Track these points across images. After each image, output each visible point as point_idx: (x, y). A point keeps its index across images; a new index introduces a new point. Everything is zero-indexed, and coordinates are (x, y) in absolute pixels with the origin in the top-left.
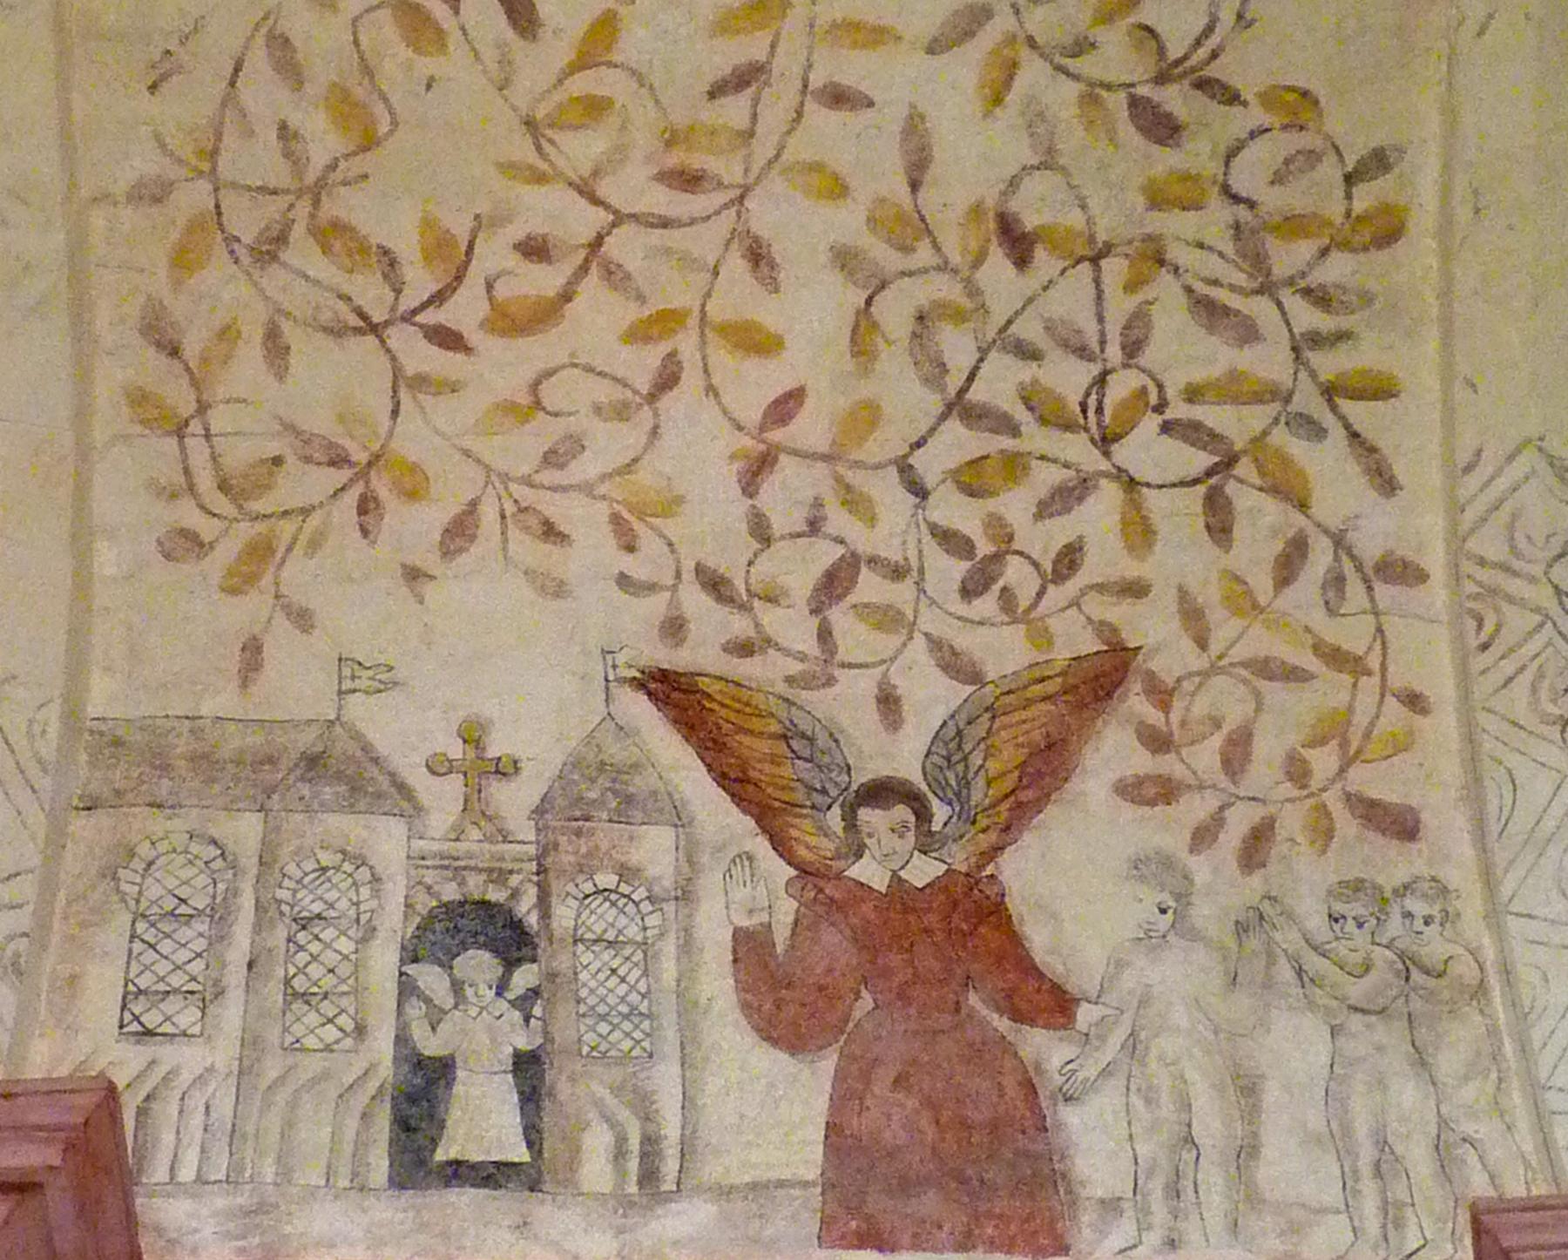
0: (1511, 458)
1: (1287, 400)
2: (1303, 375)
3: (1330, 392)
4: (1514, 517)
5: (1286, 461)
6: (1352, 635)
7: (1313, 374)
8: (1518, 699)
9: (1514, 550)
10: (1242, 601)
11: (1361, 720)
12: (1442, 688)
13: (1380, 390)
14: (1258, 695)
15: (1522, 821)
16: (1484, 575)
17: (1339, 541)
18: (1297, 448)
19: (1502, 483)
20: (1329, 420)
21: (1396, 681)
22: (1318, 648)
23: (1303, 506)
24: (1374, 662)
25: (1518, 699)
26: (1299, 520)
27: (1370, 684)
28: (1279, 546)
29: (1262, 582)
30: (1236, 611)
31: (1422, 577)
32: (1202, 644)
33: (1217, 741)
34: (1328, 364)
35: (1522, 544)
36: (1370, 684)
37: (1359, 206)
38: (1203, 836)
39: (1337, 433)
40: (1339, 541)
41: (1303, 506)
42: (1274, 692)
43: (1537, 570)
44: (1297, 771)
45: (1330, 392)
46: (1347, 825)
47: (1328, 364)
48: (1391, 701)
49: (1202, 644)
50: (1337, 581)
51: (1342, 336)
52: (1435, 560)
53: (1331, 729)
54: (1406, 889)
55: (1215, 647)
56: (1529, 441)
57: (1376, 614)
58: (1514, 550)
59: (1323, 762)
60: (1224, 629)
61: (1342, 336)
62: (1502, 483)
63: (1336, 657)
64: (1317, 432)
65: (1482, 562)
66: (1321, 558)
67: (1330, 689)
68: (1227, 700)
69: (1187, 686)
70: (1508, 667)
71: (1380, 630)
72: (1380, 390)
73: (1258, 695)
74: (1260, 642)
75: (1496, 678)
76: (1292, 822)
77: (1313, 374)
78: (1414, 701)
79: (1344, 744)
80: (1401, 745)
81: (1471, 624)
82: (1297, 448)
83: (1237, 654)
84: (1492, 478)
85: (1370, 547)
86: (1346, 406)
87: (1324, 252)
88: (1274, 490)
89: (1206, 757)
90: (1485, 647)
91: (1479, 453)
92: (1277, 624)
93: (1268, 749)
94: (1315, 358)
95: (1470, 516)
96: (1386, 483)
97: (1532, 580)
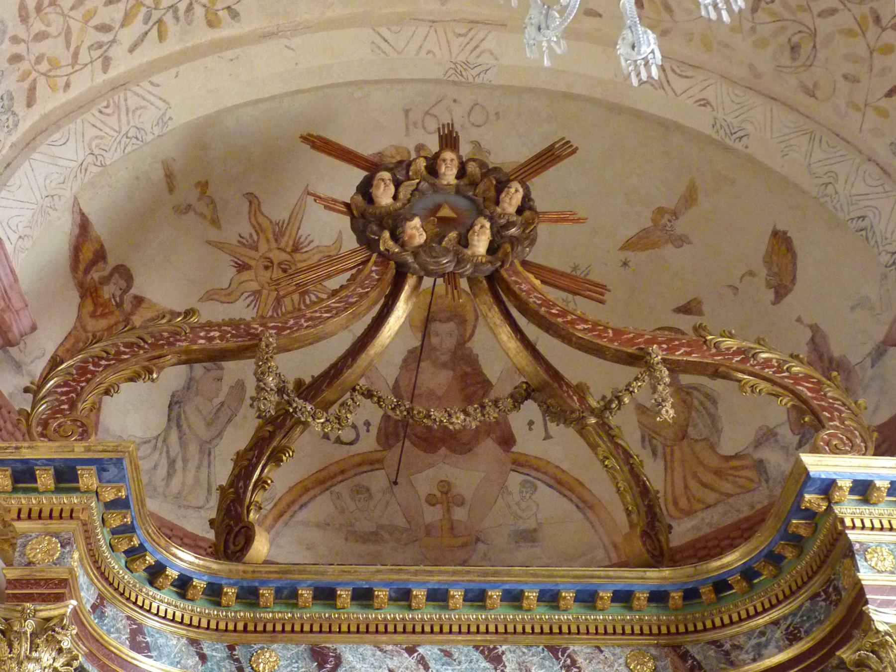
0: (161, 99)
1: (156, 9)
2: (164, 11)
3: (160, 21)
4: (144, 107)
5: (136, 15)
6: (84, 57)
7: (164, 14)
8: (91, 132)
9: (134, 111)
10: (88, 17)
11: (59, 72)
12: (73, 93)
13: (161, 37)
14: (60, 34)
15: (57, 151)
16: (122, 102)
17: (113, 41)
18: (140, 17)
19: (152, 98)
20: (151, 23)
21: (72, 77)
22: (78, 48)
23: (122, 26)
24: (77, 67)
25: (91, 132)
26: (117, 26)
27: (70, 70)
28: (108, 22)
29: (95, 22)
30: (84, 16)
31: (105, 72)
32: (71, 9)
33: (43, 28)
34: (169, 18)
35: (138, 112)
36: (70, 70)
37: (220, 13)
38: (15, 40)
39: (146, 28)
40: (113, 41)
41: (122, 26)
42: (61, 40)
43: (132, 124)
44: (39, 60)
45: (160, 21)
46: (26, 85)
47: (169, 18)
48: (66, 78)
49: (71, 9)
50: (100, 45)
51: (177, 19)
52: (112, 73)
53: (54, 64)
54: (14, 114)
55: (72, 13)
56: (168, 104)
57: (91, 62)
58: (134, 111)
59: (44, 67)
60: (78, 14)
61: (177, 19)
62: (152, 98)
63: (76, 55)
64: (146, 22)
65: (126, 100)
66: (105, 38)
67: (65, 57)
68: (56, 25)
69: (58, 10)
70: (99, 124)
71: (86, 65)
72: (161, 37)
73: (60, 34)
74: (75, 26)
75: (92, 120)
76: (24, 66)
77: (164, 14)
78: (67, 85)
79: (50, 70)
80: (53, 88)
81: (105, 104)
82: (140, 17)
83: (71, 22)
84: (153, 94)
85: (111, 53)
86: (156, 27)
87: (204, 6)
88: (126, 14)
89: (38, 26)
90: (101, 112)
91: (158, 86)
92: (82, 30)
93: (43, 47)
94: (170, 14)
95: (136, 89)
96: (131, 50)
97: (128, 123)
